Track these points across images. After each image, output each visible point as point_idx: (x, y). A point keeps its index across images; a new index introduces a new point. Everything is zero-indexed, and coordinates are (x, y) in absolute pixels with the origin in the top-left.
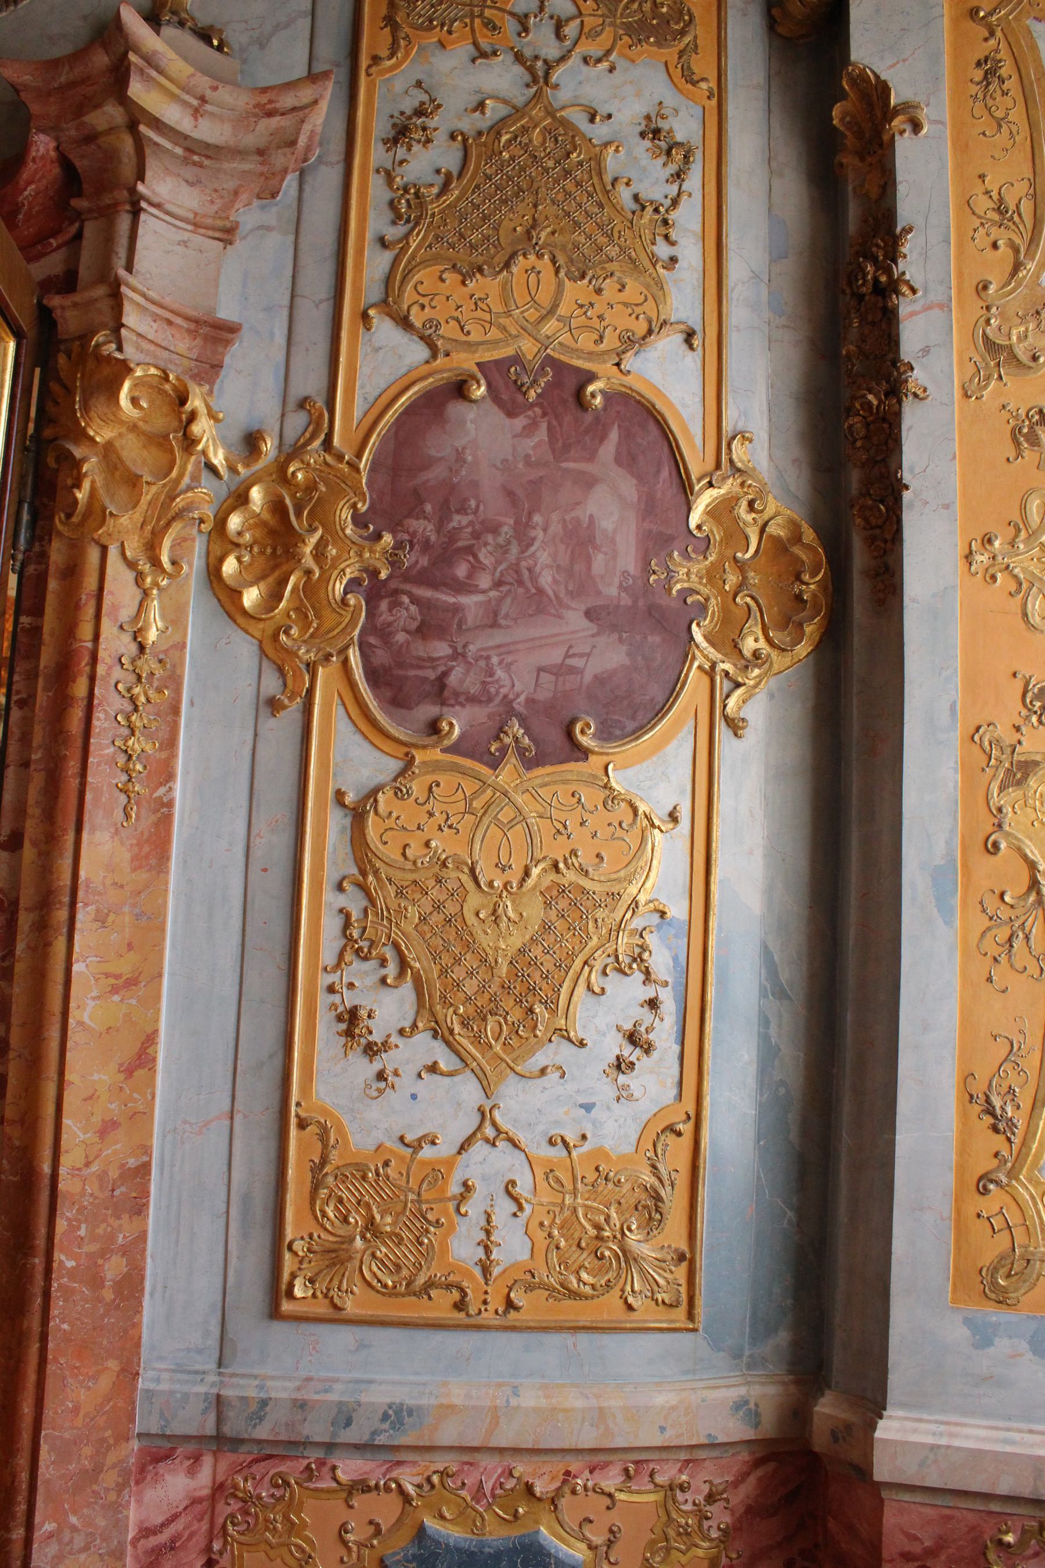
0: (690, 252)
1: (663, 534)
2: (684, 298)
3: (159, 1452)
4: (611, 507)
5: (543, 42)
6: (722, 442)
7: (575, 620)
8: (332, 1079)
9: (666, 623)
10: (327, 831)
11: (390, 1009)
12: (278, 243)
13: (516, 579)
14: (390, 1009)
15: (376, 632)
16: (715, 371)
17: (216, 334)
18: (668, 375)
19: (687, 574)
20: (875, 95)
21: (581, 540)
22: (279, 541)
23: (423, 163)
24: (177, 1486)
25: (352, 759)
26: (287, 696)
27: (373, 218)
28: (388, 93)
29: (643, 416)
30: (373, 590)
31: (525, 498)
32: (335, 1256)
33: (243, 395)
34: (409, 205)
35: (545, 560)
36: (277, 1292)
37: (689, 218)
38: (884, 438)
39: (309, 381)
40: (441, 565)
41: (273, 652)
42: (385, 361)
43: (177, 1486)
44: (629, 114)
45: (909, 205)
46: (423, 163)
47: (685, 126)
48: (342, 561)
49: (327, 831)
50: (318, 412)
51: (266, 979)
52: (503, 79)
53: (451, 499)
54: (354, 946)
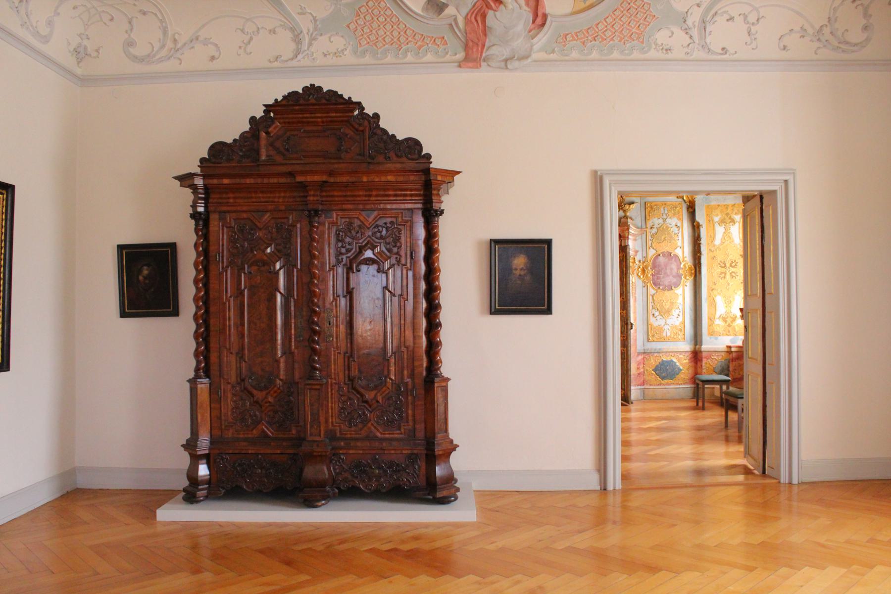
0: (680, 238)
1: (679, 268)
2: (679, 243)
3: (639, 354)
4: (674, 266)
5: (665, 216)
6: (684, 258)
7: (671, 277)
8: (652, 320)
9: (679, 276)
10: (650, 298)
11: (657, 314)
12: (640, 240)
13: (665, 273)
14: (657, 314)
15: (653, 279)
16: (684, 251)
17: (637, 252)
18: (678, 252)
19: (681, 271)
20: (698, 223)
21: (671, 269)
22: (643, 271)
23: (654, 231)
24: (640, 357)
25: (652, 291)
26: (645, 286)
27: (649, 237)
28: (649, 224)
29: (676, 256)
30: (653, 275)
31: (666, 265)
32: (653, 336)
33: (639, 257)
34: (653, 236)
35: (668, 271)
36: (648, 340)
37: (680, 235)
38: (700, 258)
39: (645, 255)
40: (658, 272)
41: (644, 282)
42: (652, 253)
43: (640, 357)
44: (674, 224)
45: (702, 236)
46: (654, 231)
47: (679, 225)
48: (650, 272)
49: (650, 298)
50: (646, 257)
51: (645, 312)
52: (661, 221)
53: (659, 266)
54: (653, 308)
